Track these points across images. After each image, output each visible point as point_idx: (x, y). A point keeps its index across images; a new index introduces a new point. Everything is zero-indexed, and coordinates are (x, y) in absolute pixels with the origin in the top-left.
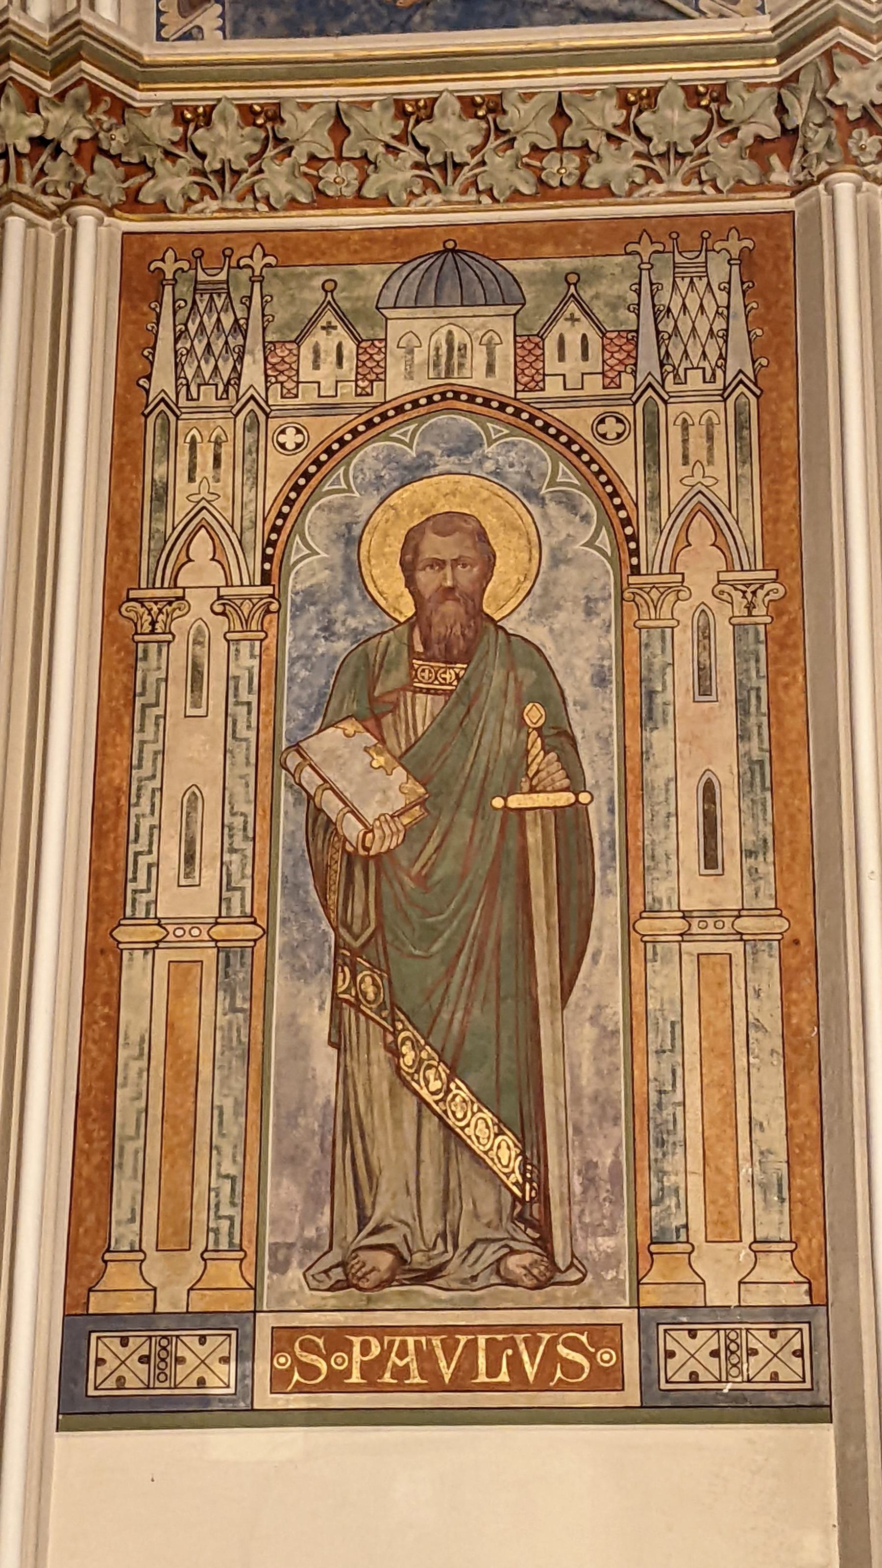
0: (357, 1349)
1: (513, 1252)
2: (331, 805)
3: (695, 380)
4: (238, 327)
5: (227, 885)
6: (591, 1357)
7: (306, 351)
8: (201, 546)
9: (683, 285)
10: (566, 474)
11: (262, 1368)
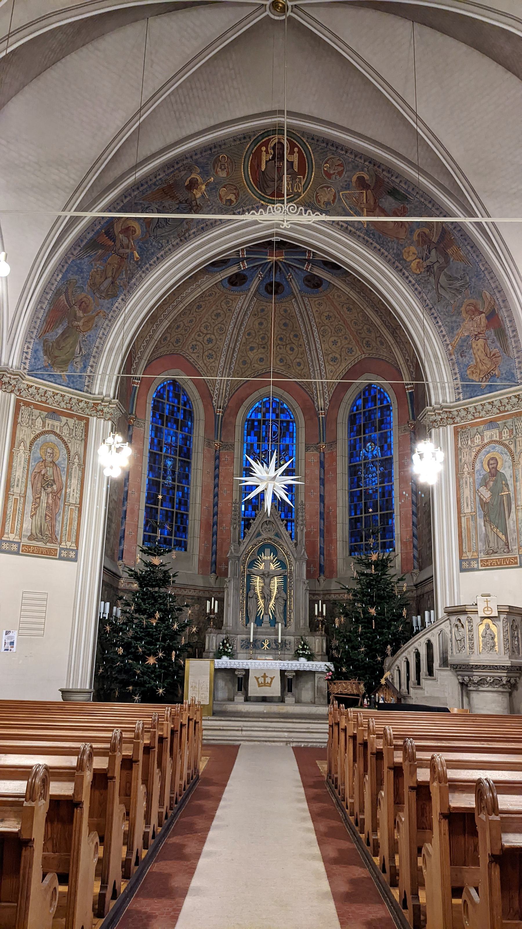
2: (482, 497)
4: (467, 437)
5: (471, 508)
8: (465, 466)
11: (480, 564)
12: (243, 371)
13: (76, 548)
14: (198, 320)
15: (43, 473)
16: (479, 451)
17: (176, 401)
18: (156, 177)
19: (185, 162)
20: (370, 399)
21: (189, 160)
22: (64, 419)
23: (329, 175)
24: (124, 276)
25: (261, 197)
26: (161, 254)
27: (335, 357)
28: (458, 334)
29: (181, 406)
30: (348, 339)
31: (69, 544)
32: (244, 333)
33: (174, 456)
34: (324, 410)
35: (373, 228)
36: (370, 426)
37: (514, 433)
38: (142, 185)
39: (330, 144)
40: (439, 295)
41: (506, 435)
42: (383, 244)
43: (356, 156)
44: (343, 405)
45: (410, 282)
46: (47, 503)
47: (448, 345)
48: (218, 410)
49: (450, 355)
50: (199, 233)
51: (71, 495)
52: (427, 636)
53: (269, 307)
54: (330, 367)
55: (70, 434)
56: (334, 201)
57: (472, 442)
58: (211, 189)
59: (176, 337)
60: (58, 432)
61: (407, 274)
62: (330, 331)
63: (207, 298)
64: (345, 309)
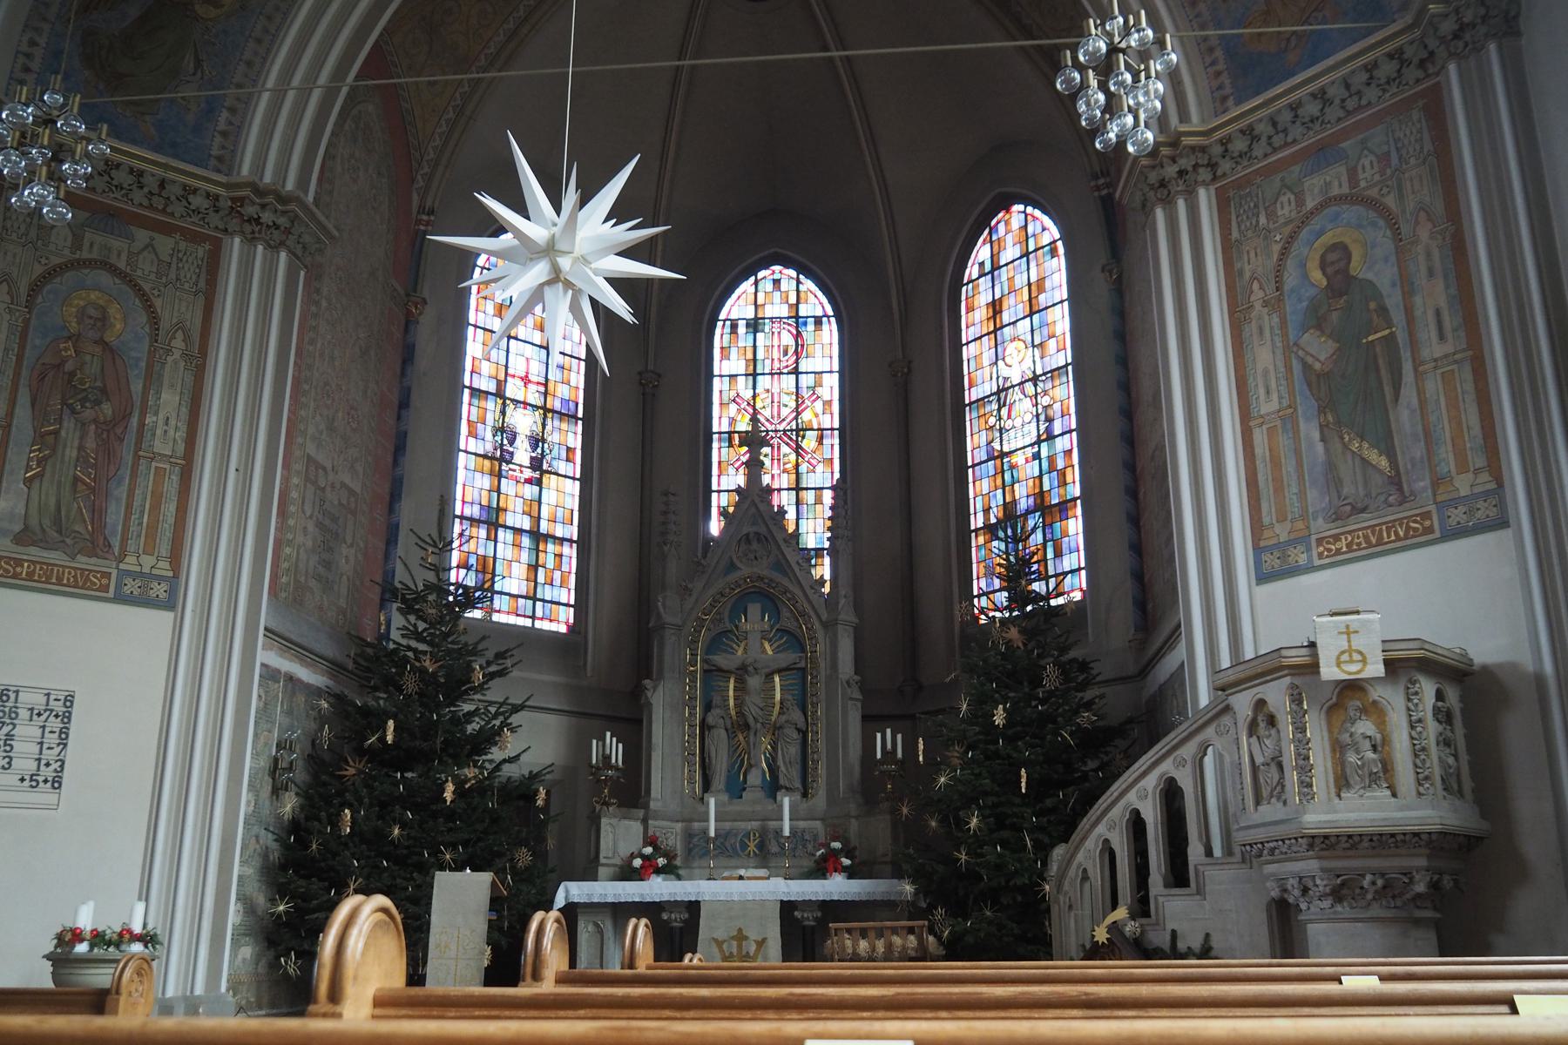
0: (1343, 540)
1: (1390, 495)
2: (1310, 360)
3: (1413, 161)
4: (1256, 206)
5: (1280, 398)
6: (1421, 524)
7: (1278, 205)
8: (1256, 286)
9: (1403, 127)
10: (1372, 214)
13: (170, 574)
15: (69, 366)
16: (1291, 240)
22: (142, 236)
31: (148, 561)
37: (1395, 161)
41: (1368, 172)
46: (81, 448)
51: (159, 432)
55: (159, 275)
57: (1271, 215)
60: (122, 265)
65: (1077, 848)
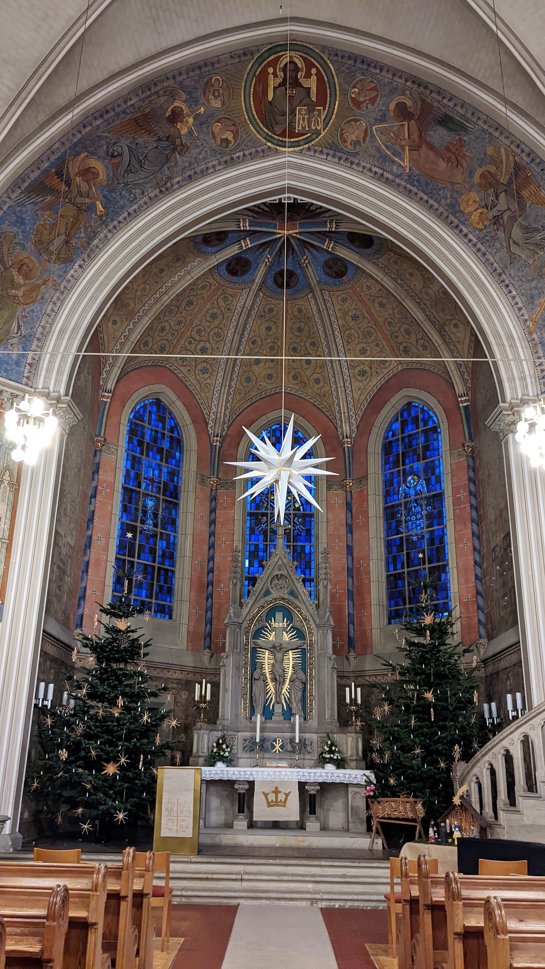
12: (247, 391)
14: (188, 322)
17: (161, 425)
18: (125, 103)
19: (165, 84)
20: (410, 422)
21: (172, 81)
23: (358, 104)
24: (83, 235)
25: (268, 138)
26: (133, 208)
27: (363, 370)
28: (540, 305)
29: (166, 432)
30: (381, 346)
32: (247, 341)
33: (157, 495)
34: (350, 438)
35: (417, 172)
36: (411, 453)
38: (107, 112)
39: (359, 61)
40: (512, 255)
42: (431, 193)
43: (394, 75)
44: (375, 430)
45: (470, 241)
47: (526, 321)
48: (215, 438)
49: (530, 333)
50: (185, 183)
52: (523, 729)
53: (278, 306)
54: (357, 383)
56: (364, 139)
58: (202, 124)
59: (160, 342)
61: (465, 230)
62: (356, 335)
63: (200, 292)
64: (376, 305)
65: (473, 766)
